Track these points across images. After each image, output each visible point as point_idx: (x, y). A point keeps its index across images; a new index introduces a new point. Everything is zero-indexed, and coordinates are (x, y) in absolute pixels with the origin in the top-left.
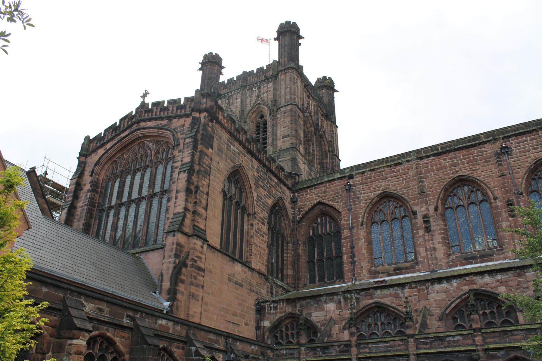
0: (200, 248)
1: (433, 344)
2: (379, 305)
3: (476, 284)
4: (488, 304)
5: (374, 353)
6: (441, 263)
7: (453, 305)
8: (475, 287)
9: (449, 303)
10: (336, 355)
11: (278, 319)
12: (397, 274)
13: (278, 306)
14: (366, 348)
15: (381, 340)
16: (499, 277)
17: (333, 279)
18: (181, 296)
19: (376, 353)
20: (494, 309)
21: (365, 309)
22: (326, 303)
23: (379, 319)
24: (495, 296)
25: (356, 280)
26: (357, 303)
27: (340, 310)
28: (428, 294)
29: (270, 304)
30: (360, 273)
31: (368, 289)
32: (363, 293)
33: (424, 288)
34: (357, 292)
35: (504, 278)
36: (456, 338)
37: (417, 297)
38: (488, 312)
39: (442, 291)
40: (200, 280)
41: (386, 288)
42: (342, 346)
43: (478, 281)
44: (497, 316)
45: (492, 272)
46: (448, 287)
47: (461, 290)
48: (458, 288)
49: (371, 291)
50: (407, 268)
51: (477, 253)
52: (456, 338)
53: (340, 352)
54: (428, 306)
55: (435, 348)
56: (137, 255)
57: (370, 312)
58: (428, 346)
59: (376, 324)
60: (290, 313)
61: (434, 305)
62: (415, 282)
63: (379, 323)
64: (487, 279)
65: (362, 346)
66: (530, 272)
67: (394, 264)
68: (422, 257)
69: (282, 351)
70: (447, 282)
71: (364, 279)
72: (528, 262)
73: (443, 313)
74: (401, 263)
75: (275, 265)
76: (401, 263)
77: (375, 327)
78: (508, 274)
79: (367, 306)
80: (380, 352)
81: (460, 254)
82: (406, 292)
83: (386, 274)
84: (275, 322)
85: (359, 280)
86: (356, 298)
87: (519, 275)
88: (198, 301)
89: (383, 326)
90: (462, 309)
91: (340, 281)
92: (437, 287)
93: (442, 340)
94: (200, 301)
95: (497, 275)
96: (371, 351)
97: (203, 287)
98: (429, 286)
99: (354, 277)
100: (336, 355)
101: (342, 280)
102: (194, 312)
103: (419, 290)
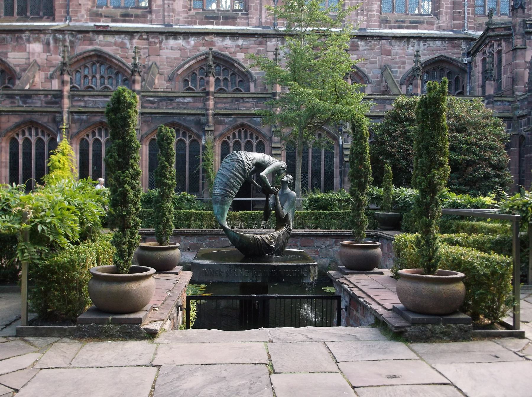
1: (161, 103)
2: (99, 54)
3: (214, 46)
4: (223, 70)
5: (91, 107)
6: (178, 17)
7: (187, 66)
8: (214, 49)
9: (183, 62)
10: (41, 107)
12: (124, 21)
14: (80, 101)
15: (100, 93)
16: (240, 42)
17: (39, 15)
19: (93, 107)
20: (228, 76)
21: (81, 57)
22: (29, 41)
23: (98, 70)
24: (232, 62)
25: (70, 20)
26: (72, 47)
27: (48, 54)
28: (160, 49)
30: (76, 12)
31: (87, 32)
32: (80, 36)
33: (157, 41)
34: (72, 34)
35: (245, 44)
36: (187, 100)
37: (146, 51)
38: (221, 78)
39: (177, 48)
41: (110, 35)
42: (50, 96)
43: (218, 43)
44: (230, 83)
45: (234, 35)
46: (184, 44)
47: (198, 50)
48: (195, 47)
49: (91, 35)
50: (137, 16)
51: (220, 12)
52: (187, 100)
53: (47, 103)
54: (158, 63)
55: (162, 109)
57: (87, 61)
58: (154, 105)
59: (94, 77)
61: (165, 63)
62: (147, 33)
63: (98, 76)
64: (228, 42)
65: (76, 98)
66: (271, 42)
67: (122, 8)
68: (157, 6)
70: (184, 39)
71: (81, 21)
72: (271, 31)
73: (173, 73)
74: (131, 8)
76: (131, 8)
77: (92, 80)
78: (250, 41)
79: (85, 52)
80: (98, 107)
81: (201, 11)
82: (134, 43)
83: (110, 19)
85: (74, 20)
86: (71, 42)
87: (260, 44)
89: (102, 79)
90: (195, 72)
91: (48, 18)
92: (172, 42)
93: (172, 100)
95: (238, 39)
96: (87, 106)
98: (163, 40)
99: (67, 16)
100: (41, 107)
101: (51, 18)
103: (151, 43)
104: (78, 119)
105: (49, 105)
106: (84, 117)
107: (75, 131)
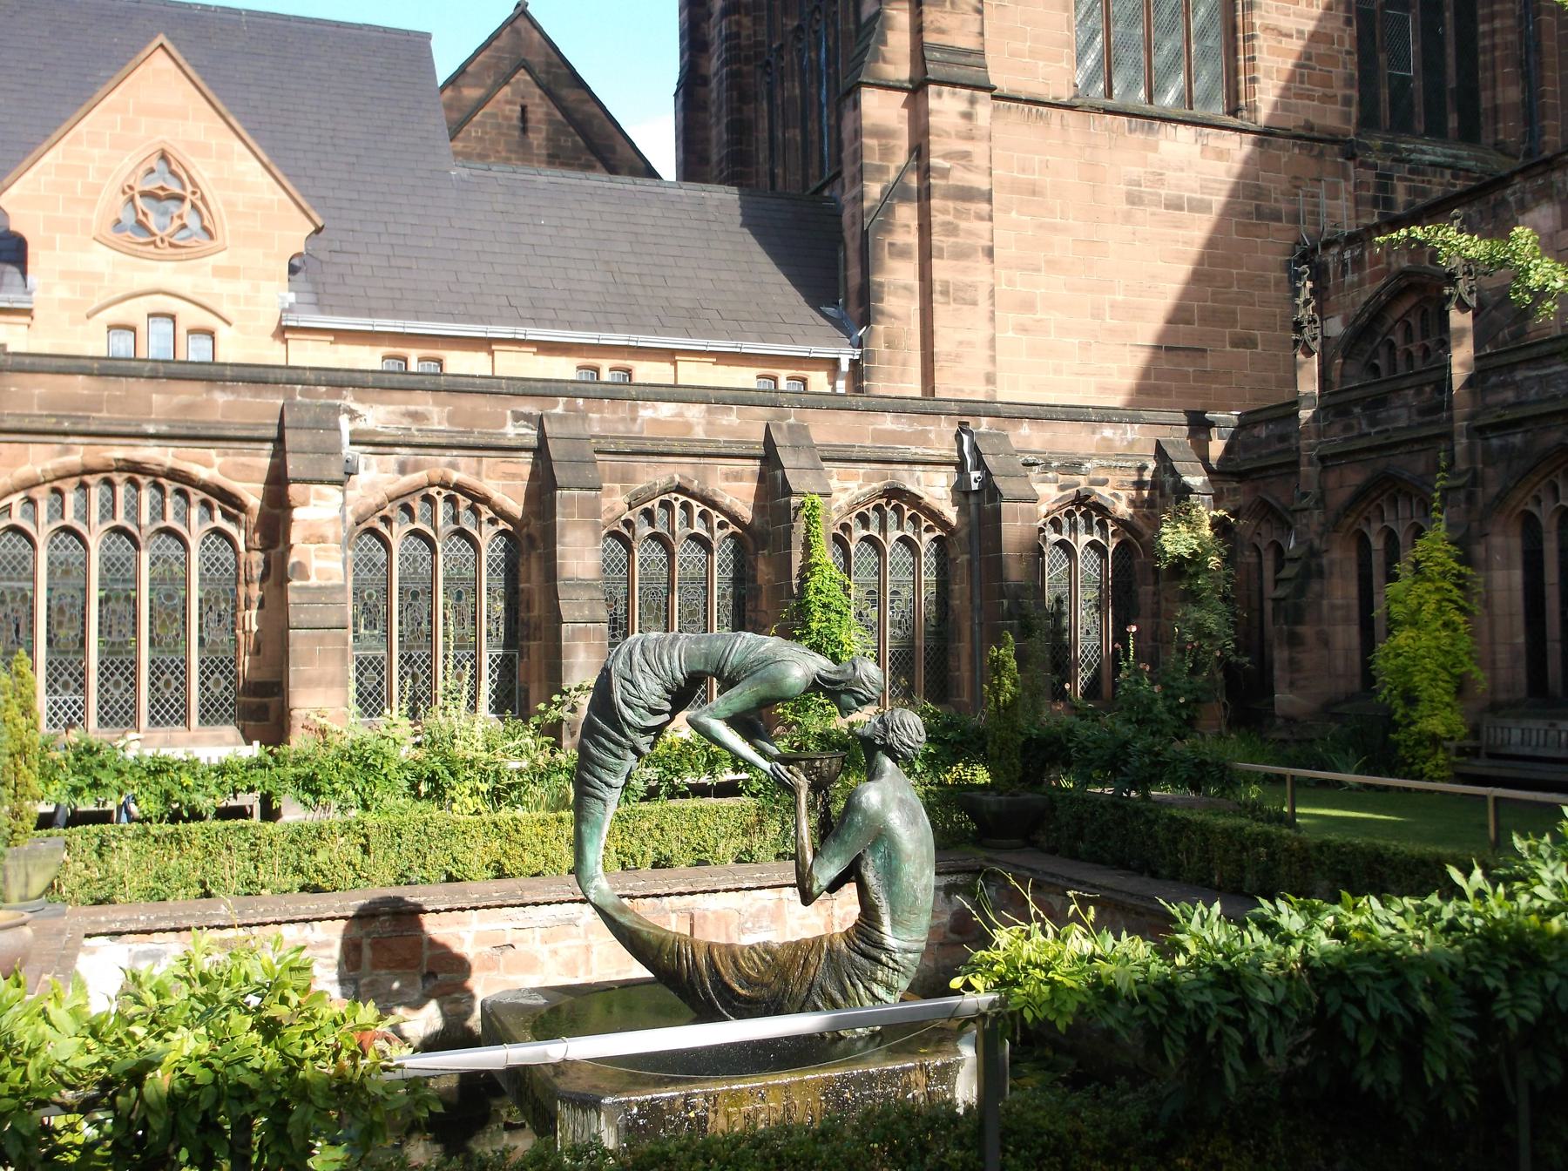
0: (961, 122)
11: (1367, 303)
13: (1367, 254)
14: (1504, 385)
18: (903, 302)
29: (1341, 253)
40: (970, 233)
42: (1428, 389)
53: (1422, 412)
56: (826, 193)
60: (1404, 273)
69: (1256, 431)
75: (1417, 85)
84: (1358, 316)
88: (974, 303)
94: (984, 305)
96: (1523, 398)
97: (990, 252)
102: (961, 343)
104: (1503, 449)
105: (1428, 419)
106: (1517, 439)
107: (1493, 490)
